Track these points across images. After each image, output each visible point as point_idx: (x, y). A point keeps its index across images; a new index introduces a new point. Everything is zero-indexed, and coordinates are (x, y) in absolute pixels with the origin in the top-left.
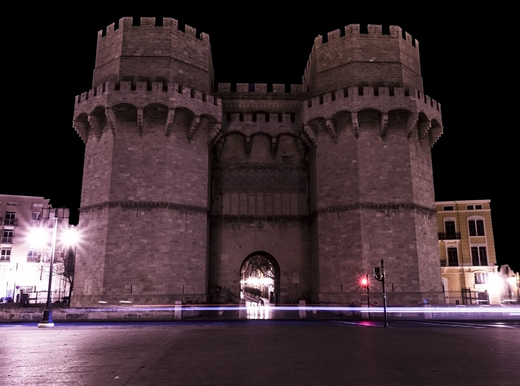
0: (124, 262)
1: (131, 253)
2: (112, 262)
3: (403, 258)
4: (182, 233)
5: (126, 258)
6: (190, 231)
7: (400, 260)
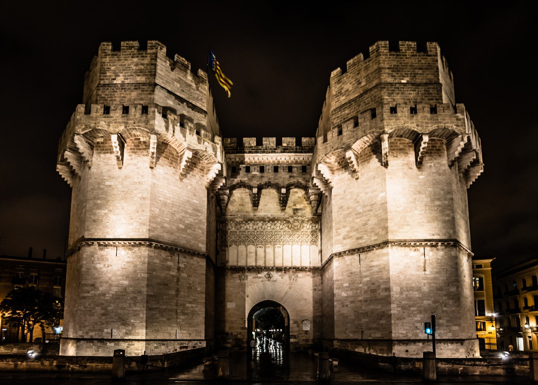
0: (102, 304)
1: (111, 295)
2: (89, 304)
3: (441, 301)
4: (173, 276)
5: (105, 300)
6: (184, 275)
7: (437, 304)
